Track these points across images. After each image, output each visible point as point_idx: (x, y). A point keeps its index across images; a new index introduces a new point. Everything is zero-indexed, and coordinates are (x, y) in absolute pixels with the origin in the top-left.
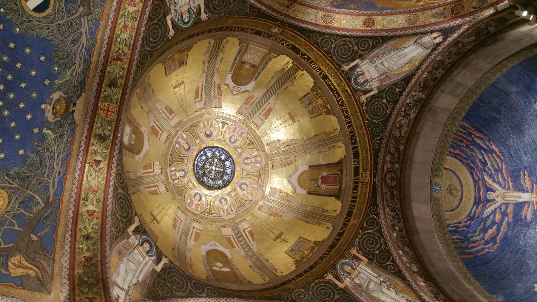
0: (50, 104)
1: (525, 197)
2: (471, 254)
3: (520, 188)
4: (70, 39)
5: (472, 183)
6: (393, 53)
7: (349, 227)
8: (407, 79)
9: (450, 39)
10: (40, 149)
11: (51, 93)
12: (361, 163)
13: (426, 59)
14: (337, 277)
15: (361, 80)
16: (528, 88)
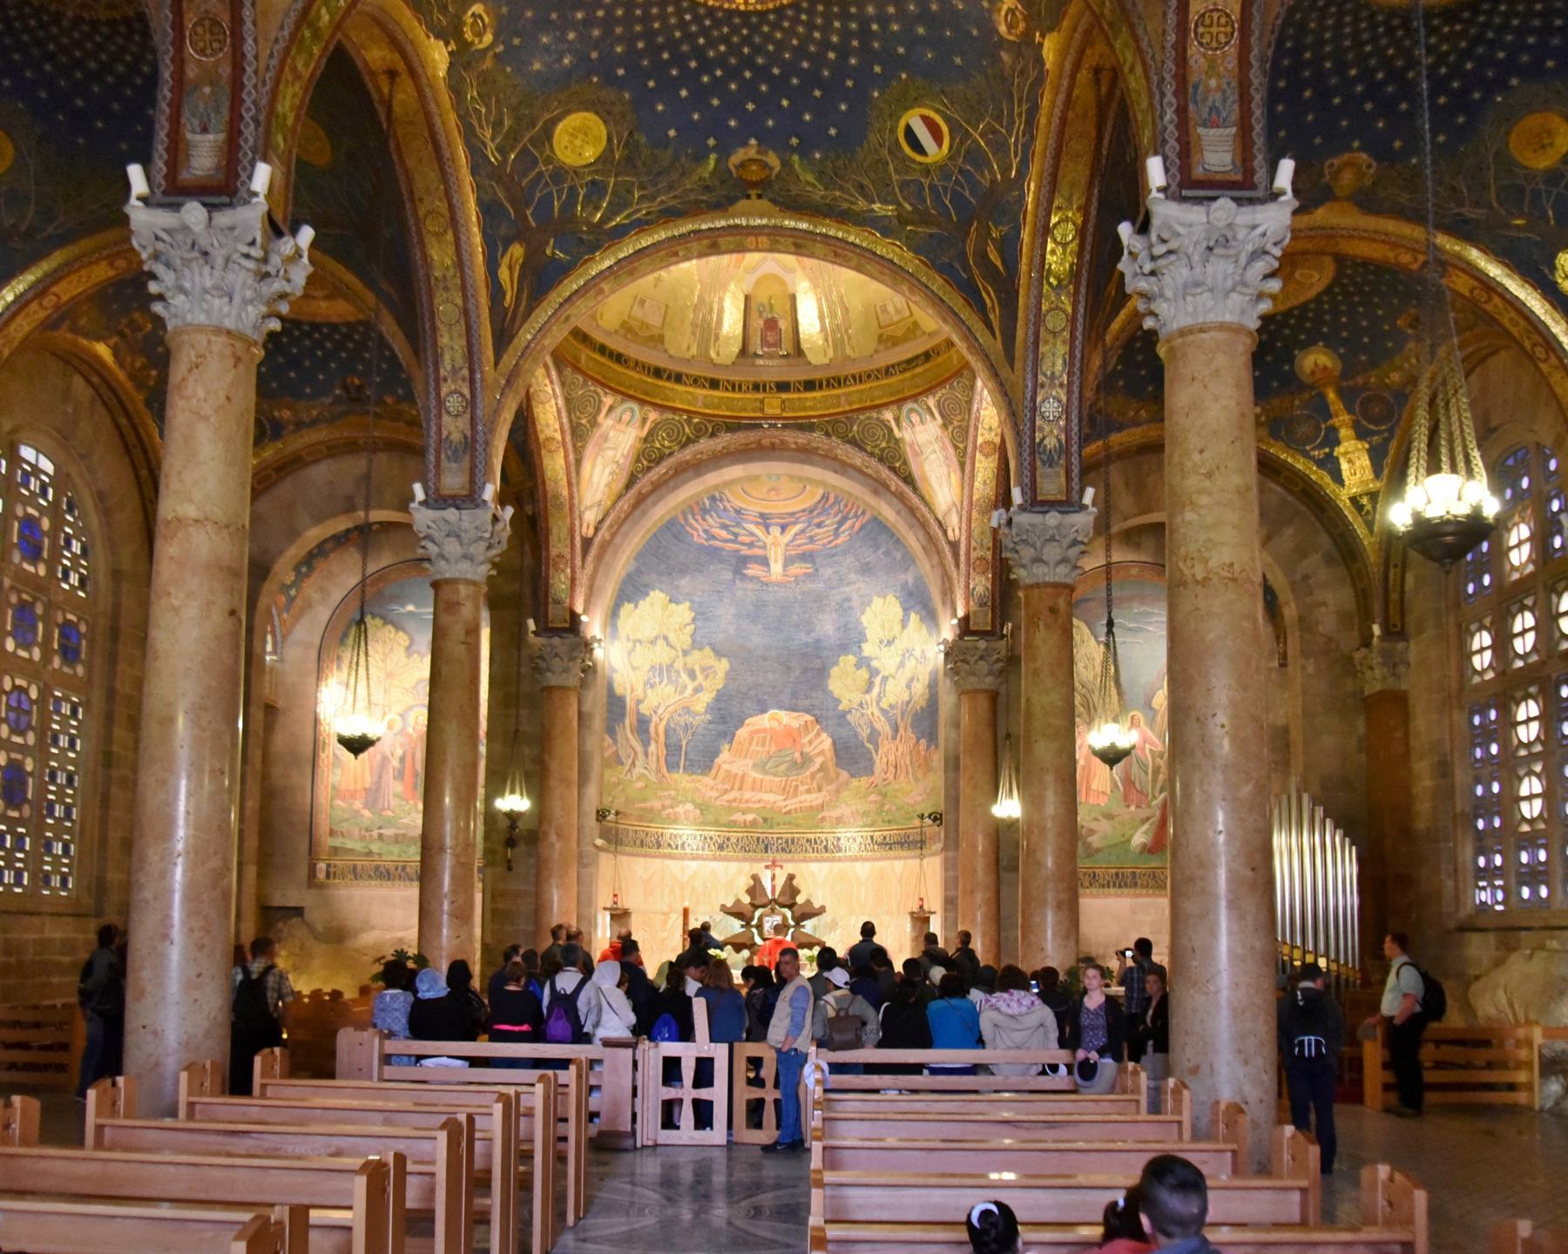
0: (758, 152)
1: (777, 568)
2: (686, 520)
3: (788, 561)
4: (866, 181)
5: (790, 510)
6: (945, 469)
7: (691, 389)
8: (909, 480)
9: (947, 550)
10: (683, 159)
11: (776, 151)
12: (796, 396)
13: (932, 511)
14: (611, 409)
15: (915, 417)
16: (910, 594)
